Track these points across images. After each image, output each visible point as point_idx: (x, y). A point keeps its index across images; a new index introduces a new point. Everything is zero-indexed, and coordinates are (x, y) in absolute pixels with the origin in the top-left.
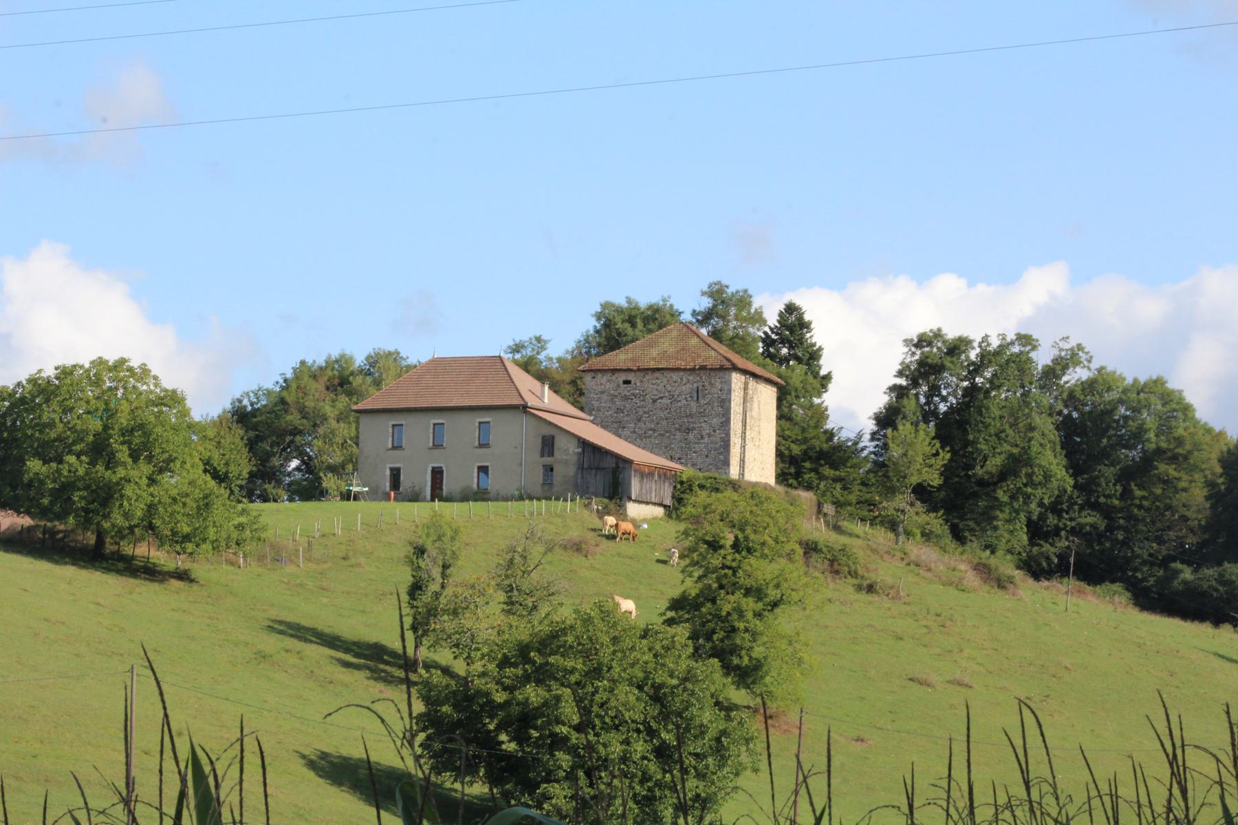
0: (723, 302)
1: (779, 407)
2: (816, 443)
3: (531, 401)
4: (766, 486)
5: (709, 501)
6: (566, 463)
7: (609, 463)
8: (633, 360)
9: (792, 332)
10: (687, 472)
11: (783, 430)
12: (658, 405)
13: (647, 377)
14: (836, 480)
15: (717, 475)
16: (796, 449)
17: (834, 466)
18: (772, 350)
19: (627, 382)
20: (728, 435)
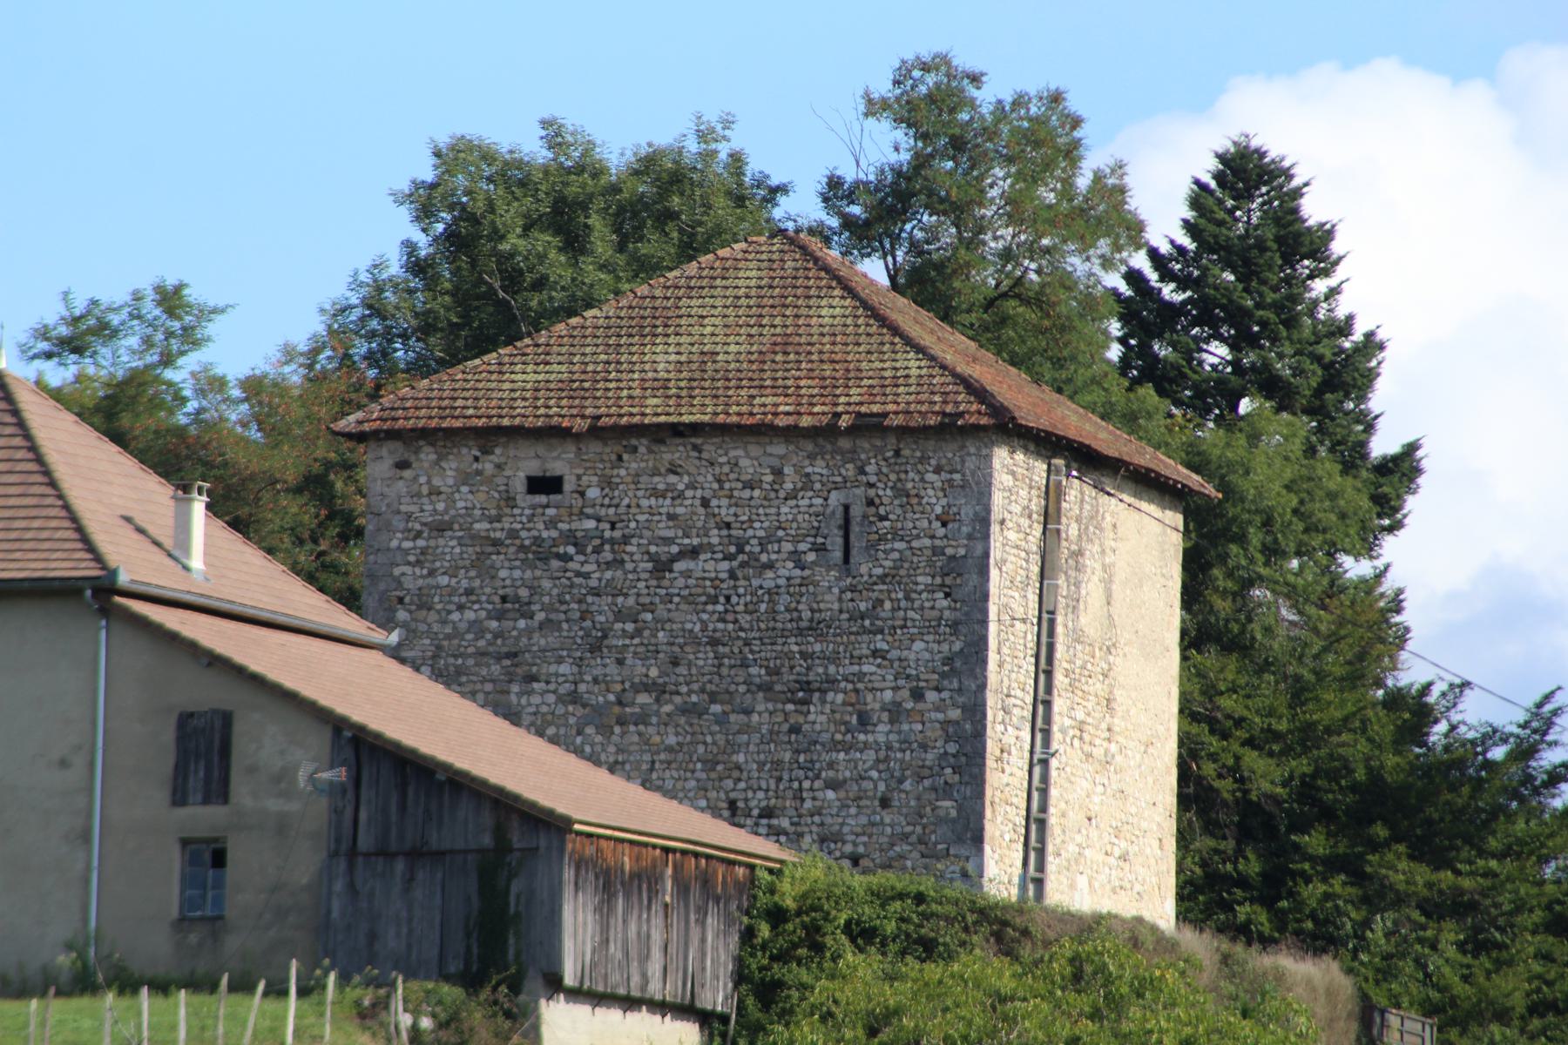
0: (958, 145)
1: (1192, 595)
2: (1354, 748)
3: (133, 564)
4: (1137, 933)
5: (891, 995)
6: (282, 827)
7: (467, 831)
8: (569, 389)
9: (1248, 274)
10: (801, 869)
11: (1211, 692)
12: (676, 582)
13: (632, 464)
14: (1437, 908)
15: (927, 884)
16: (1267, 776)
17: (1430, 851)
18: (1162, 350)
19: (544, 485)
20: (976, 712)
